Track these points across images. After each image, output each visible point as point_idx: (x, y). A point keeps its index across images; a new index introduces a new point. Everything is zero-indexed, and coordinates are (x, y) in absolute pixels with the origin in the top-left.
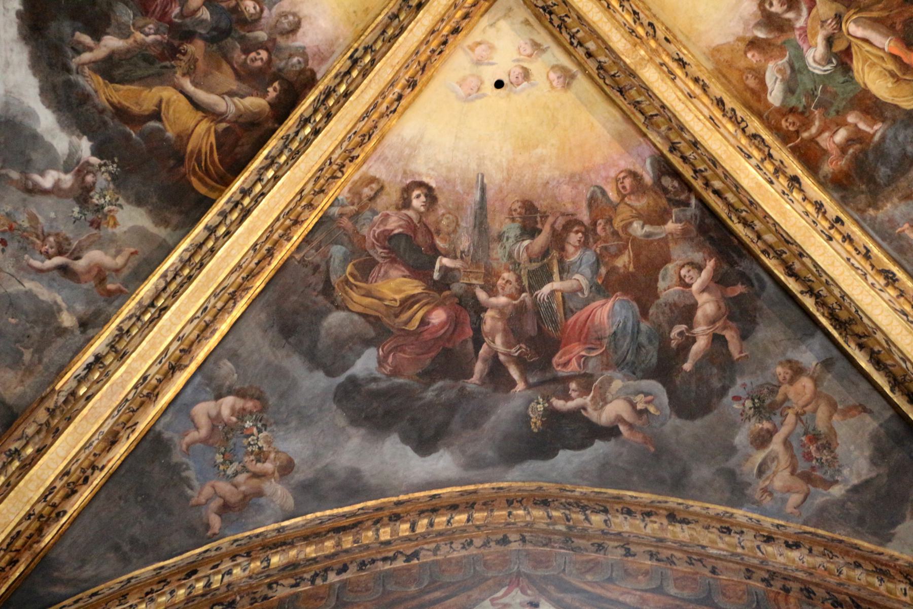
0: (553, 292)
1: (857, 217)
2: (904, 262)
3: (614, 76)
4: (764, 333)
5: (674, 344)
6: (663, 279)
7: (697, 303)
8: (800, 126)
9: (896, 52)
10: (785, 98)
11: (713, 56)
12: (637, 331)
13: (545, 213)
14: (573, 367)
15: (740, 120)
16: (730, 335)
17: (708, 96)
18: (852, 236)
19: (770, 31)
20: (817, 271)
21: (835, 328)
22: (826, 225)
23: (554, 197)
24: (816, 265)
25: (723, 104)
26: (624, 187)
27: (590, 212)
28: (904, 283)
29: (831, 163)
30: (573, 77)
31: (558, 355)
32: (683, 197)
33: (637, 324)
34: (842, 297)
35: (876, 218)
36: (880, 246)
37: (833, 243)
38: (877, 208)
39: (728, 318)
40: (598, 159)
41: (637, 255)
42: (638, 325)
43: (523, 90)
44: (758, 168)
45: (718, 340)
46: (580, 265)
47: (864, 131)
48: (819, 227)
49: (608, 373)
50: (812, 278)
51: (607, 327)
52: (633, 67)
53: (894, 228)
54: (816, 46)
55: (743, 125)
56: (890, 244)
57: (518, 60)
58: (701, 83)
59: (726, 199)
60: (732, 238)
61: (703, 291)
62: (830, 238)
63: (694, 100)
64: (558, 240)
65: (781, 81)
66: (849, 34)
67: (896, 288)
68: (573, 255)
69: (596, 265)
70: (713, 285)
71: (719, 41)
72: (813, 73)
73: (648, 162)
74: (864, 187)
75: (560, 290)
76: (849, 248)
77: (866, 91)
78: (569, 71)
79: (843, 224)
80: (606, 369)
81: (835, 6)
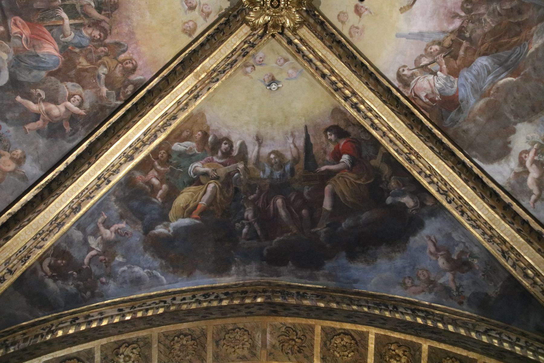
0: (62, 19)
1: (110, 191)
2: (86, 216)
3: (191, 59)
4: (42, 142)
5: (33, 91)
6: (73, 85)
7: (58, 105)
8: (161, 160)
9: (199, 208)
10: (176, 152)
11: (199, 113)
12: (39, 68)
13: (111, 16)
14: (14, 30)
15: (165, 128)
16: (40, 123)
17: (178, 112)
18: (100, 189)
19: (212, 143)
20: (80, 173)
21: (46, 182)
22: (106, 176)
23: (121, 23)
24: (84, 172)
25: (174, 119)
26: (127, 63)
27: (112, 43)
28: (73, 217)
29: (141, 177)
30: (190, 35)
31: (22, 20)
32: (122, 97)
33: (44, 69)
34: (65, 186)
35: (111, 201)
36: (94, 204)
37: (97, 180)
38: (115, 202)
39: (50, 122)
40: (143, 49)
41: (86, 70)
42: (44, 70)
43: (183, 5)
44: (139, 139)
45: (37, 116)
46: (80, 37)
47: (158, 193)
48: (105, 173)
49: (11, 50)
50: (76, 169)
51: (42, 51)
52: (195, 71)
53: (104, 211)
54: (203, 167)
55: (162, 130)
56: (96, 209)
57: (200, 4)
58: (185, 107)
59: (121, 121)
60: (98, 124)
61: (66, 108)
62: (99, 178)
63: (176, 104)
64: (96, 24)
65: (186, 150)
66: (209, 184)
67: (70, 213)
68: (86, 32)
69: (80, 46)
70: (70, 114)
71: (208, 116)
72: (189, 166)
73: (142, 77)
74: (127, 194)
75: (64, 23)
76: (94, 188)
77: (179, 193)
78: (194, 33)
79: (107, 184)
80: (14, 50)
81: (223, 176)
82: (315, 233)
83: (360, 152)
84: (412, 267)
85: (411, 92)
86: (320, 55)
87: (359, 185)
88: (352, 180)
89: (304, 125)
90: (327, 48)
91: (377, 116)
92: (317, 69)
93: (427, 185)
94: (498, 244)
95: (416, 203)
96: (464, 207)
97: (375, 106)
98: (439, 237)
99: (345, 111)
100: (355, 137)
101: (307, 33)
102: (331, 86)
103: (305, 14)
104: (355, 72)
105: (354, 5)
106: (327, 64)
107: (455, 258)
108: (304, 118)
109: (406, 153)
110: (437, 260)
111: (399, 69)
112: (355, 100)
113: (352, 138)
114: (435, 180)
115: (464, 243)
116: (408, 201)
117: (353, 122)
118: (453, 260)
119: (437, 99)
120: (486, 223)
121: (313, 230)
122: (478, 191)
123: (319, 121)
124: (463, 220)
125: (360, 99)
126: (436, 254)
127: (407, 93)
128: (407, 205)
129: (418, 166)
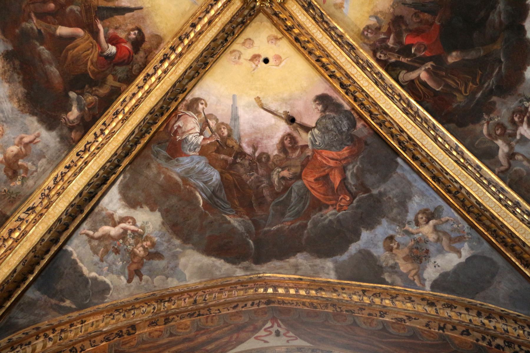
82: (30, 17)
83: (120, 64)
84: (4, 119)
85: (182, 112)
86: (216, 20)
87: (87, 64)
88: (91, 57)
89: (143, 6)
90: (223, 27)
91: (159, 79)
92: (200, 19)
93: (93, 132)
94: (41, 202)
95: (73, 122)
96: (76, 168)
97: (170, 76)
98: (40, 146)
99: (159, 49)
100: (134, 58)
101: (237, 6)
102: (184, 33)
103: (252, 6)
104: (201, 56)
105: (260, 53)
106: (208, 27)
107: (20, 163)
108: (149, 6)
109: (123, 109)
110: (15, 145)
111: (204, 100)
112: (173, 57)
113: (133, 57)
114: (100, 139)
115: (36, 171)
116: (74, 114)
117: (149, 57)
118: (17, 161)
119: (178, 137)
120: (64, 189)
121: (33, 15)
122: (95, 179)
123: (148, 22)
124: (61, 169)
125: (176, 61)
126: (21, 144)
127: (181, 109)
128: (70, 113)
129: (112, 122)
